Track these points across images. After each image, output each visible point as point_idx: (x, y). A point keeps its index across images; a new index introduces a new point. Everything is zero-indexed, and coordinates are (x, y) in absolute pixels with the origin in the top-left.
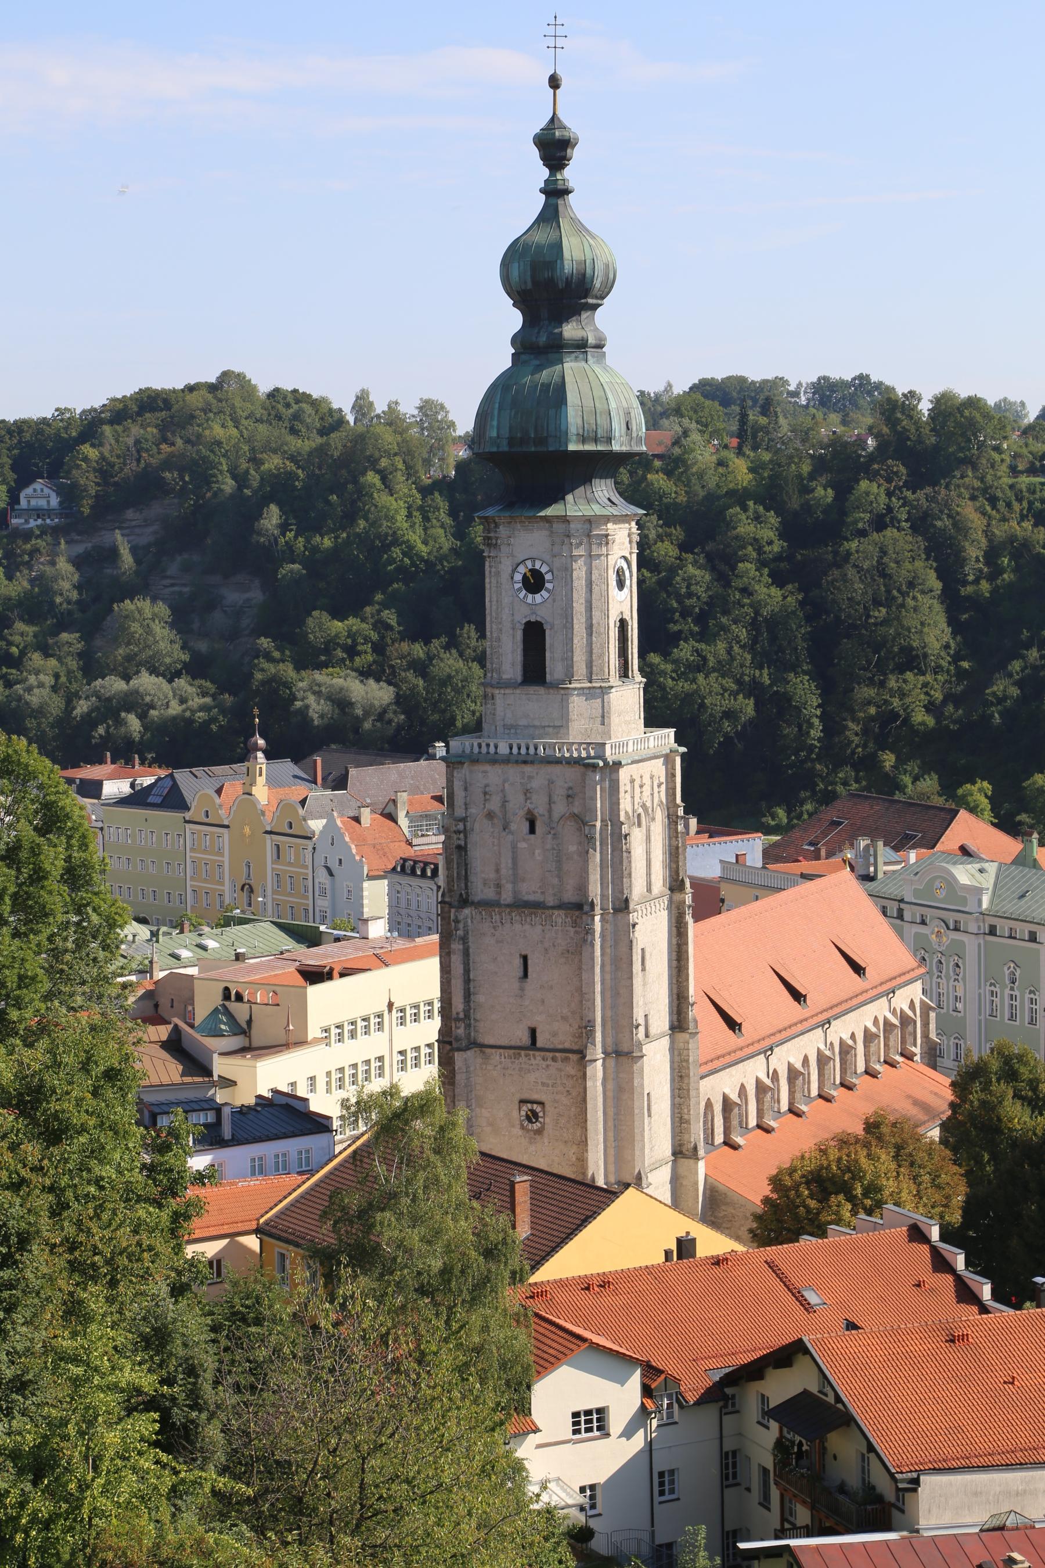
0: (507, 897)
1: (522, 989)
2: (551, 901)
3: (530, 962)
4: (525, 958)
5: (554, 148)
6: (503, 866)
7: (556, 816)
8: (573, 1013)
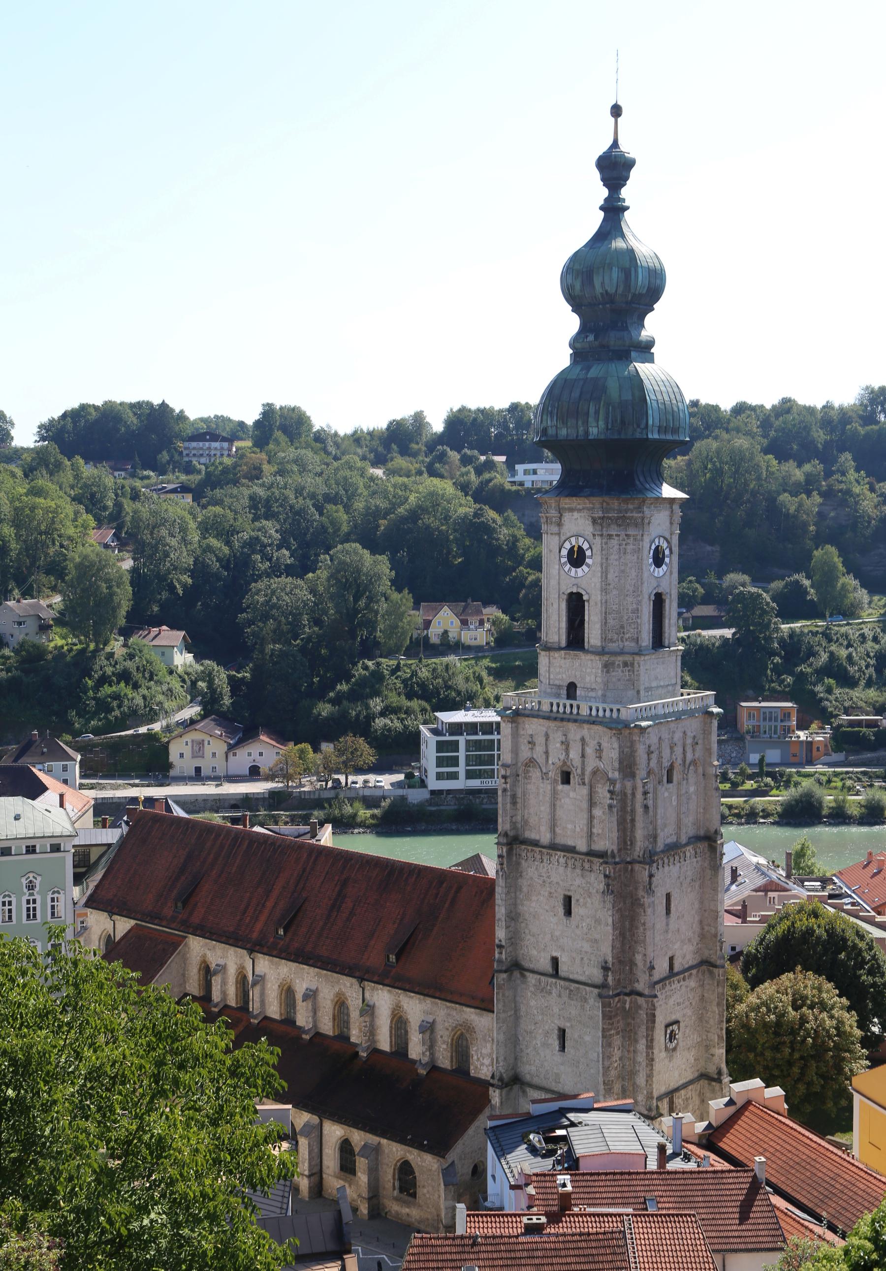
0: (660, 846)
1: (667, 925)
2: (684, 840)
3: (672, 899)
4: (668, 896)
5: (614, 168)
6: (659, 817)
7: (687, 762)
8: (694, 933)
